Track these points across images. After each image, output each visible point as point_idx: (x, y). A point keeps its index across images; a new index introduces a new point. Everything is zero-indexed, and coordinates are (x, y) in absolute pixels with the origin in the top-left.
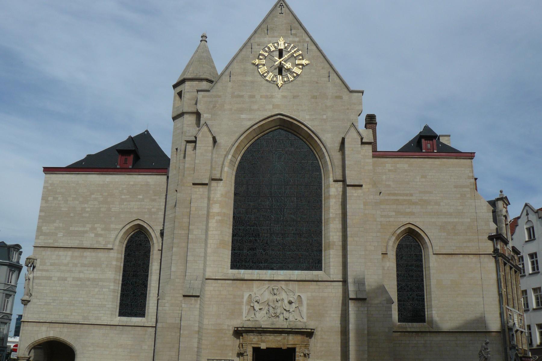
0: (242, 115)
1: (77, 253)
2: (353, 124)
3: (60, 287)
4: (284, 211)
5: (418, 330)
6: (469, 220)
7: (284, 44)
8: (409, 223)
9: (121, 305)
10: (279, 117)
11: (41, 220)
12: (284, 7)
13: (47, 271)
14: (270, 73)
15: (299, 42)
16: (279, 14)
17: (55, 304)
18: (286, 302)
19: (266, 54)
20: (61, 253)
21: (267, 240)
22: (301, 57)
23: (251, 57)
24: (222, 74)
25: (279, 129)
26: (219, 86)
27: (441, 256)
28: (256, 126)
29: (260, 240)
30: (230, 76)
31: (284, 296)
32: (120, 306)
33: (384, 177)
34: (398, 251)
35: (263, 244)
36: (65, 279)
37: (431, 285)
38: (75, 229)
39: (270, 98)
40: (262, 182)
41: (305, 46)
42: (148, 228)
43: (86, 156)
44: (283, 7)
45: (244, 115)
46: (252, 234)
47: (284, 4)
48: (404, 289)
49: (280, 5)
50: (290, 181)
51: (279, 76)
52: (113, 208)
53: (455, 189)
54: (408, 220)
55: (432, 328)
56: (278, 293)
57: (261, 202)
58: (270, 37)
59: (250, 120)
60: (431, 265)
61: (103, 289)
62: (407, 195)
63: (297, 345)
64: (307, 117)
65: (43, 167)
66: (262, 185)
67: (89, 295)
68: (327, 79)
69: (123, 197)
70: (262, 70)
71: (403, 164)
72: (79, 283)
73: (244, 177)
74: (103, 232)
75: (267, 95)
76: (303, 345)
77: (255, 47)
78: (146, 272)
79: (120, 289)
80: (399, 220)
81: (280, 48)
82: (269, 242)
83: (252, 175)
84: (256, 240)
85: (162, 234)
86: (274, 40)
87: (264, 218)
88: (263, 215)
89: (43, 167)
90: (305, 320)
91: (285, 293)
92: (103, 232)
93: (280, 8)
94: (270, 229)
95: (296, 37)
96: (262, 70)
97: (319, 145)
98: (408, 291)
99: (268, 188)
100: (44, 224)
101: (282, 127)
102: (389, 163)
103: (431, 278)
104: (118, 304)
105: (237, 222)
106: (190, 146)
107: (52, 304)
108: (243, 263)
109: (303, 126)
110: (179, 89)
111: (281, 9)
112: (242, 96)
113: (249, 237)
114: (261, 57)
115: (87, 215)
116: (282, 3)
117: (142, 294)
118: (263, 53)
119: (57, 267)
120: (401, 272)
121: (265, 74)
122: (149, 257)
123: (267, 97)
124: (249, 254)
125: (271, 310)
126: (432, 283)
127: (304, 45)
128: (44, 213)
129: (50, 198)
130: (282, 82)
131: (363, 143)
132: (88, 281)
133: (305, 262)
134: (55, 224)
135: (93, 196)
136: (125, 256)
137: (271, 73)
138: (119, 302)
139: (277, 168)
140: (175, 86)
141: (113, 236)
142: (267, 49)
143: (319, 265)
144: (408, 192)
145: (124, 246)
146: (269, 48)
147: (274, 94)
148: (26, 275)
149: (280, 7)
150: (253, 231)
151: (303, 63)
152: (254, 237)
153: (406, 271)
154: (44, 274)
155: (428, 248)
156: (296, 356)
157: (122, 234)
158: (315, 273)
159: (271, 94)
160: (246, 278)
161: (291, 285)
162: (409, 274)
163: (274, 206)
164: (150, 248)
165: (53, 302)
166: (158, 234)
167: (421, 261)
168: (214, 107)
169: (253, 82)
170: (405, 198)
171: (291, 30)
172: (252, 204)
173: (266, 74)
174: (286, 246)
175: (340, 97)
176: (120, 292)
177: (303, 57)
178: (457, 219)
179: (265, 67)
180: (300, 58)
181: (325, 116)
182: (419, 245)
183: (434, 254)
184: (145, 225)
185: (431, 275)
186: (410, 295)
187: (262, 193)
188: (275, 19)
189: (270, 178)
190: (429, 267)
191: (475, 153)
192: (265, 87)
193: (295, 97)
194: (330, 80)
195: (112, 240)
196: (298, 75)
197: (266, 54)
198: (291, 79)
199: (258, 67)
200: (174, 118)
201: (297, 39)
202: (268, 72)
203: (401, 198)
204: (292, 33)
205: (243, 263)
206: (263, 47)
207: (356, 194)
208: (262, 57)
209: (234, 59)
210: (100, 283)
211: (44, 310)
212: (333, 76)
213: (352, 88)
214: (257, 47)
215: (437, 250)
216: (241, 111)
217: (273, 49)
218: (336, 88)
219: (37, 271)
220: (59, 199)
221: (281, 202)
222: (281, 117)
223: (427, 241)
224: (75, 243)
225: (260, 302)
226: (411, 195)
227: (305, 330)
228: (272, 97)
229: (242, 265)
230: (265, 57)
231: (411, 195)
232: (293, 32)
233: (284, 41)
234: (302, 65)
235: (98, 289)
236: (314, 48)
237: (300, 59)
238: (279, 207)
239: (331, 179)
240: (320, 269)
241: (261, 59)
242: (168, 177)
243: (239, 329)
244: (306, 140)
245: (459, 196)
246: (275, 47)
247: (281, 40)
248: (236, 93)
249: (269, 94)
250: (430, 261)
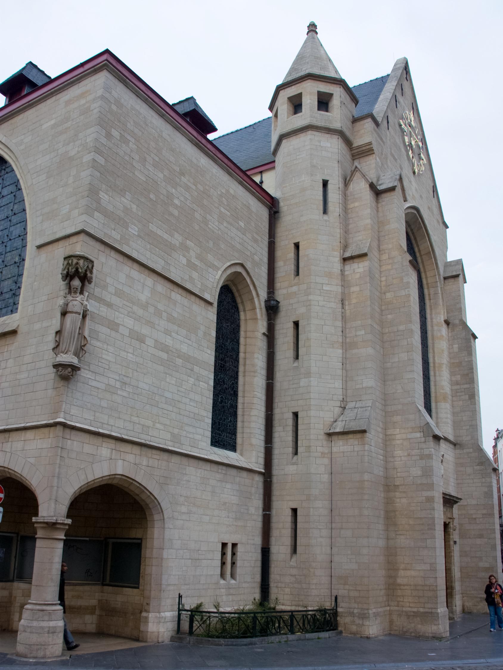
1: (162, 287)
13: (109, 305)
17: (125, 394)
20: (135, 273)
36: (141, 339)
61: (201, 383)
67: (180, 389)
72: (164, 356)
117: (232, 406)
119: (128, 304)
132: (179, 357)
211: (104, 404)
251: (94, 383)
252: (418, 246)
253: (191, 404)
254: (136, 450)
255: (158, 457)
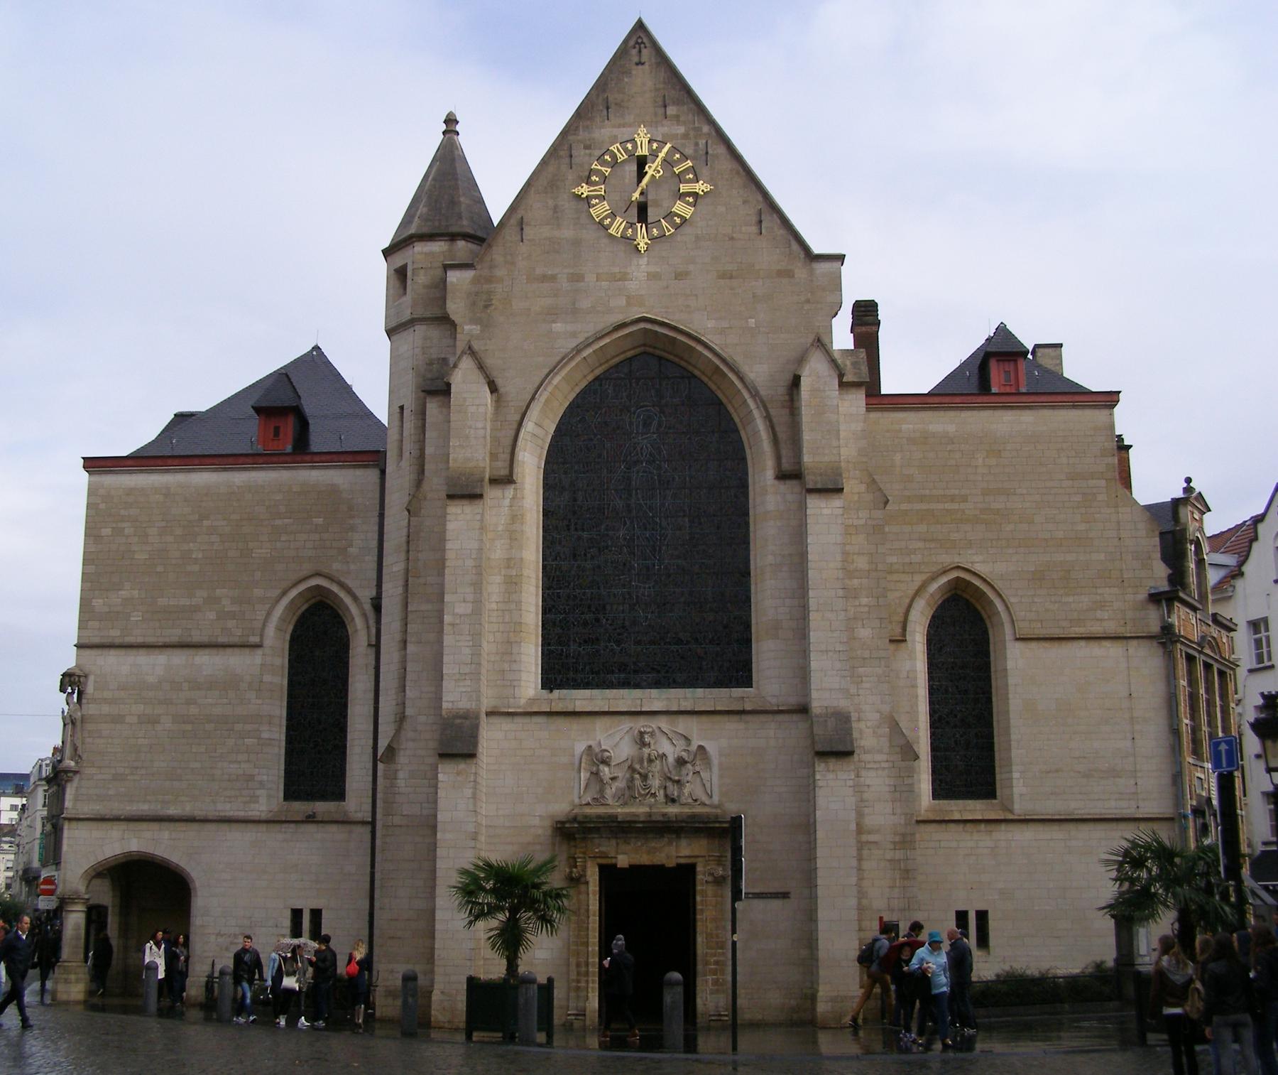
0: (554, 325)
2: (819, 340)
3: (145, 738)
4: (660, 551)
5: (980, 818)
6: (1102, 557)
7: (649, 142)
8: (958, 567)
9: (289, 774)
10: (642, 325)
11: (89, 584)
12: (645, 47)
14: (618, 218)
15: (686, 136)
16: (635, 67)
18: (671, 759)
19: (607, 171)
21: (624, 619)
22: (691, 176)
23: (570, 178)
24: (501, 222)
25: (645, 353)
26: (497, 254)
27: (1034, 645)
28: (590, 351)
29: (607, 620)
30: (522, 229)
31: (665, 747)
32: (285, 777)
33: (898, 457)
34: (932, 632)
35: (615, 629)
36: (154, 721)
37: (1011, 713)
38: (171, 603)
39: (619, 280)
40: (607, 483)
41: (700, 146)
42: (342, 594)
43: (173, 416)
44: (642, 46)
45: (559, 325)
46: (589, 607)
47: (645, 40)
48: (947, 722)
49: (637, 43)
50: (674, 479)
51: (639, 225)
52: (257, 551)
53: (1071, 482)
54: (956, 560)
55: (1011, 811)
56: (652, 742)
57: (607, 530)
58: (614, 126)
59: (574, 335)
60: (1010, 664)
62: (952, 499)
63: (700, 859)
64: (710, 324)
65: (83, 458)
66: (607, 489)
68: (754, 229)
69: (278, 522)
70: (600, 210)
71: (943, 423)
72: (189, 727)
73: (565, 473)
74: (235, 608)
75: (612, 274)
76: (711, 858)
77: (579, 153)
78: (342, 698)
79: (283, 738)
80: (935, 560)
81: (639, 152)
82: (627, 623)
83: (584, 467)
84: (597, 620)
85: (377, 606)
86: (624, 133)
87: (615, 567)
88: (612, 563)
89: (83, 458)
90: (716, 799)
91: (669, 741)
92: (235, 608)
93: (637, 50)
94: (629, 593)
95: (678, 125)
96: (600, 210)
97: (739, 391)
98: (955, 726)
99: (621, 497)
100: (97, 592)
101: (651, 350)
102: (910, 422)
103: (1011, 696)
104: (282, 773)
105: (553, 580)
106: (432, 407)
107: (129, 777)
108: (571, 675)
109: (700, 348)
110: (399, 260)
111: (640, 51)
112: (553, 278)
113: (583, 613)
114: (594, 178)
115: (196, 568)
116: (642, 35)
118: (599, 167)
120: (939, 681)
121: (607, 222)
122: (347, 663)
123: (613, 278)
124: (583, 652)
125: (638, 782)
126: (1012, 708)
127: (697, 144)
128: (94, 567)
129: (106, 531)
130: (647, 240)
131: (843, 385)
133: (712, 668)
134: (120, 592)
135: (206, 523)
136: (289, 660)
137: (619, 219)
138: (283, 767)
139: (642, 449)
140: (387, 253)
141: (261, 616)
142: (607, 157)
143: (745, 674)
144: (957, 492)
145: (288, 637)
146: (614, 156)
147: (629, 270)
148: (63, 712)
149: (637, 46)
150: (591, 600)
151: (697, 191)
152: (594, 613)
153: (951, 681)
154: (106, 709)
155: (1002, 624)
156: (698, 883)
157: (281, 611)
158: (737, 692)
159: (622, 270)
160: (577, 709)
161: (683, 725)
162: (957, 687)
163: (638, 537)
164: (348, 640)
165: (132, 774)
166: (368, 607)
167: (987, 654)
168: (486, 307)
169: (577, 243)
170: (948, 506)
171: (665, 106)
172: (585, 535)
173: (609, 220)
174: (668, 632)
175: (788, 274)
176: (283, 743)
177: (696, 175)
178: (1074, 554)
179: (605, 202)
180: (687, 177)
181: (753, 320)
182: (982, 620)
183: (1017, 639)
184: (335, 588)
185: (1011, 689)
186: (961, 736)
187: (608, 509)
188: (626, 80)
189: (625, 472)
190: (1006, 670)
191: (1120, 392)
192: (607, 253)
193: (679, 276)
194: (763, 231)
195: (258, 625)
196: (684, 220)
197: (607, 171)
198: (669, 231)
199: (589, 203)
200: (390, 332)
201: (681, 130)
202: (613, 215)
203: (940, 506)
204: (668, 113)
205: (571, 675)
206: (598, 153)
207: (826, 511)
208: (597, 179)
209: (529, 184)
210: (238, 727)
212: (769, 221)
213: (817, 249)
214: (583, 152)
215: (1024, 628)
216: (552, 314)
217: (622, 157)
218: (778, 250)
219: (88, 703)
220: (126, 531)
221: (653, 529)
222: (649, 326)
223: (1000, 609)
224: (174, 635)
225: (613, 764)
226: (964, 499)
227: (717, 825)
228: (624, 277)
229: (568, 679)
230: (605, 179)
231: (964, 499)
232: (671, 110)
233: (649, 136)
234: (695, 195)
235: (233, 740)
236: (721, 150)
237: (690, 181)
238: (649, 541)
239: (770, 473)
240: (747, 682)
241: (595, 184)
242: (383, 472)
243: (567, 825)
244: (710, 379)
245: (1078, 498)
246: (626, 150)
247: (642, 135)
248: (539, 271)
249: (616, 270)
250: (1009, 655)
251: (100, 777)
252: (694, 366)
253: (232, 766)
254: (155, 826)
255: (184, 829)
